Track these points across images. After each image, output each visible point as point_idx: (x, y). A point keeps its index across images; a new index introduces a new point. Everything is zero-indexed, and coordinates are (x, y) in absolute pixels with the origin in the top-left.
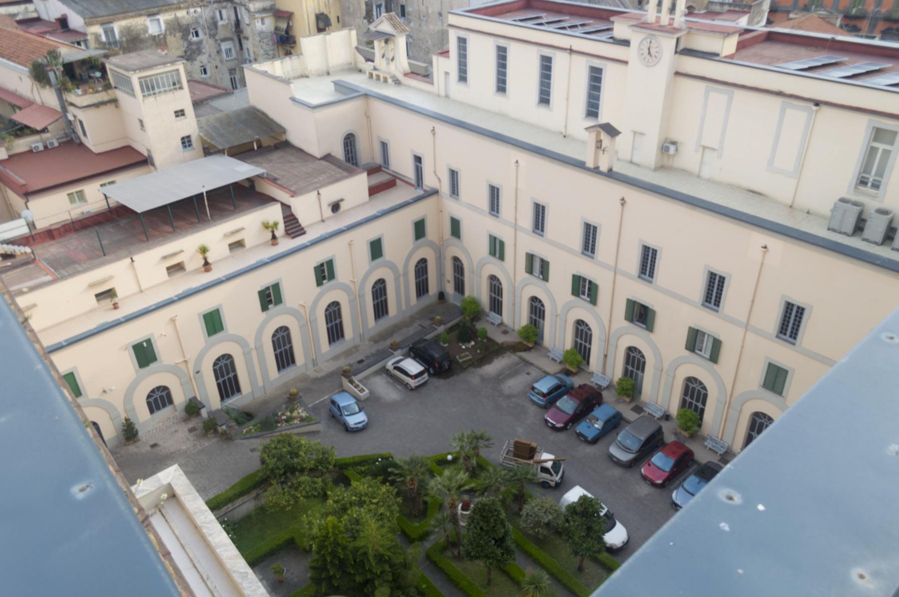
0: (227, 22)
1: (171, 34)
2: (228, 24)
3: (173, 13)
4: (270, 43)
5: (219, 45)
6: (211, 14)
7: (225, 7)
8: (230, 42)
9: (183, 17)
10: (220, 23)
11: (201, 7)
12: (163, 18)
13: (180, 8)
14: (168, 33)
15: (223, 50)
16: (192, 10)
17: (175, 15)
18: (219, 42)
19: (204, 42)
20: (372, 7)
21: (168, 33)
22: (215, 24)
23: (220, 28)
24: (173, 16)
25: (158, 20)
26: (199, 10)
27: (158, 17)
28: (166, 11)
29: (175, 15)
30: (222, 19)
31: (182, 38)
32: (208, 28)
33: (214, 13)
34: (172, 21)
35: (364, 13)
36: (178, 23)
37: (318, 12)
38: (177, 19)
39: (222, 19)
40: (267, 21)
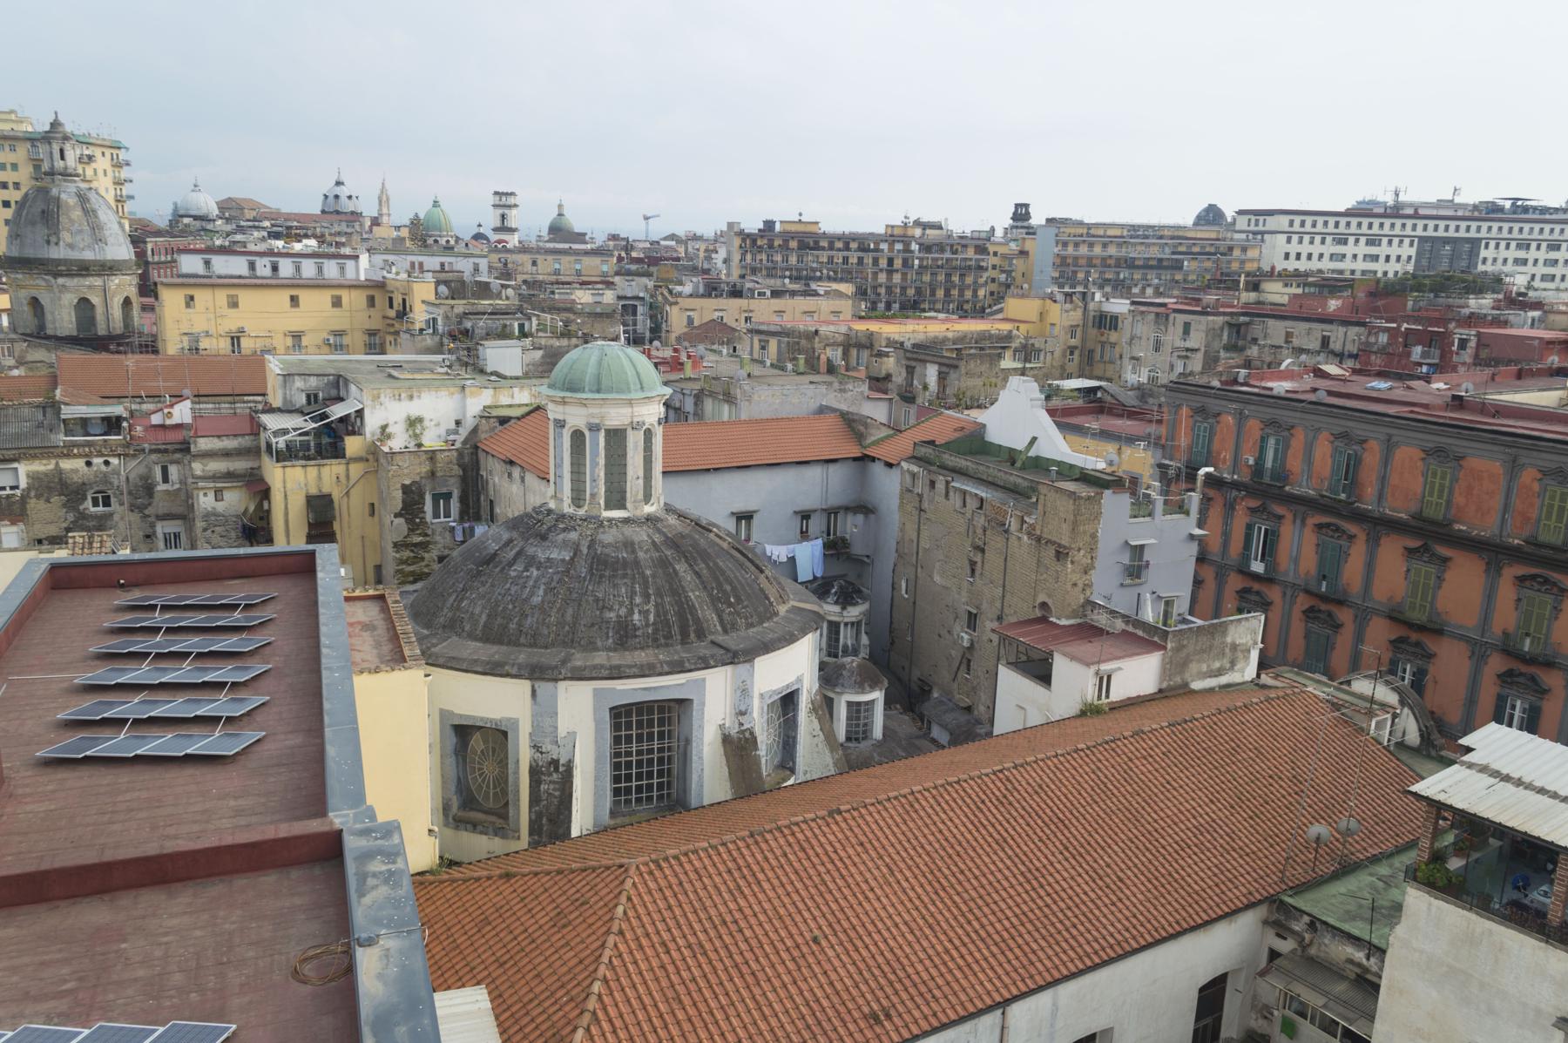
0: (177, 486)
1: (38, 497)
2: (179, 489)
3: (53, 461)
4: (233, 534)
5: (153, 526)
6: (142, 470)
7: (172, 462)
8: (179, 522)
9: (76, 471)
10: (161, 487)
11: (119, 455)
12: (24, 469)
13: (68, 456)
14: (33, 494)
15: (160, 535)
16: (98, 461)
17: (57, 464)
18: (152, 519)
19: (116, 517)
20: (422, 496)
21: (33, 494)
22: (149, 489)
23: (156, 495)
24: (51, 467)
25: (16, 469)
26: (114, 461)
27: (15, 465)
28: (34, 457)
29: (57, 464)
30: (166, 479)
31: (64, 506)
32: (130, 493)
33: (150, 470)
34: (46, 475)
35: (398, 504)
36: (61, 479)
37: (314, 491)
38: (58, 469)
39: (166, 479)
40: (227, 495)
